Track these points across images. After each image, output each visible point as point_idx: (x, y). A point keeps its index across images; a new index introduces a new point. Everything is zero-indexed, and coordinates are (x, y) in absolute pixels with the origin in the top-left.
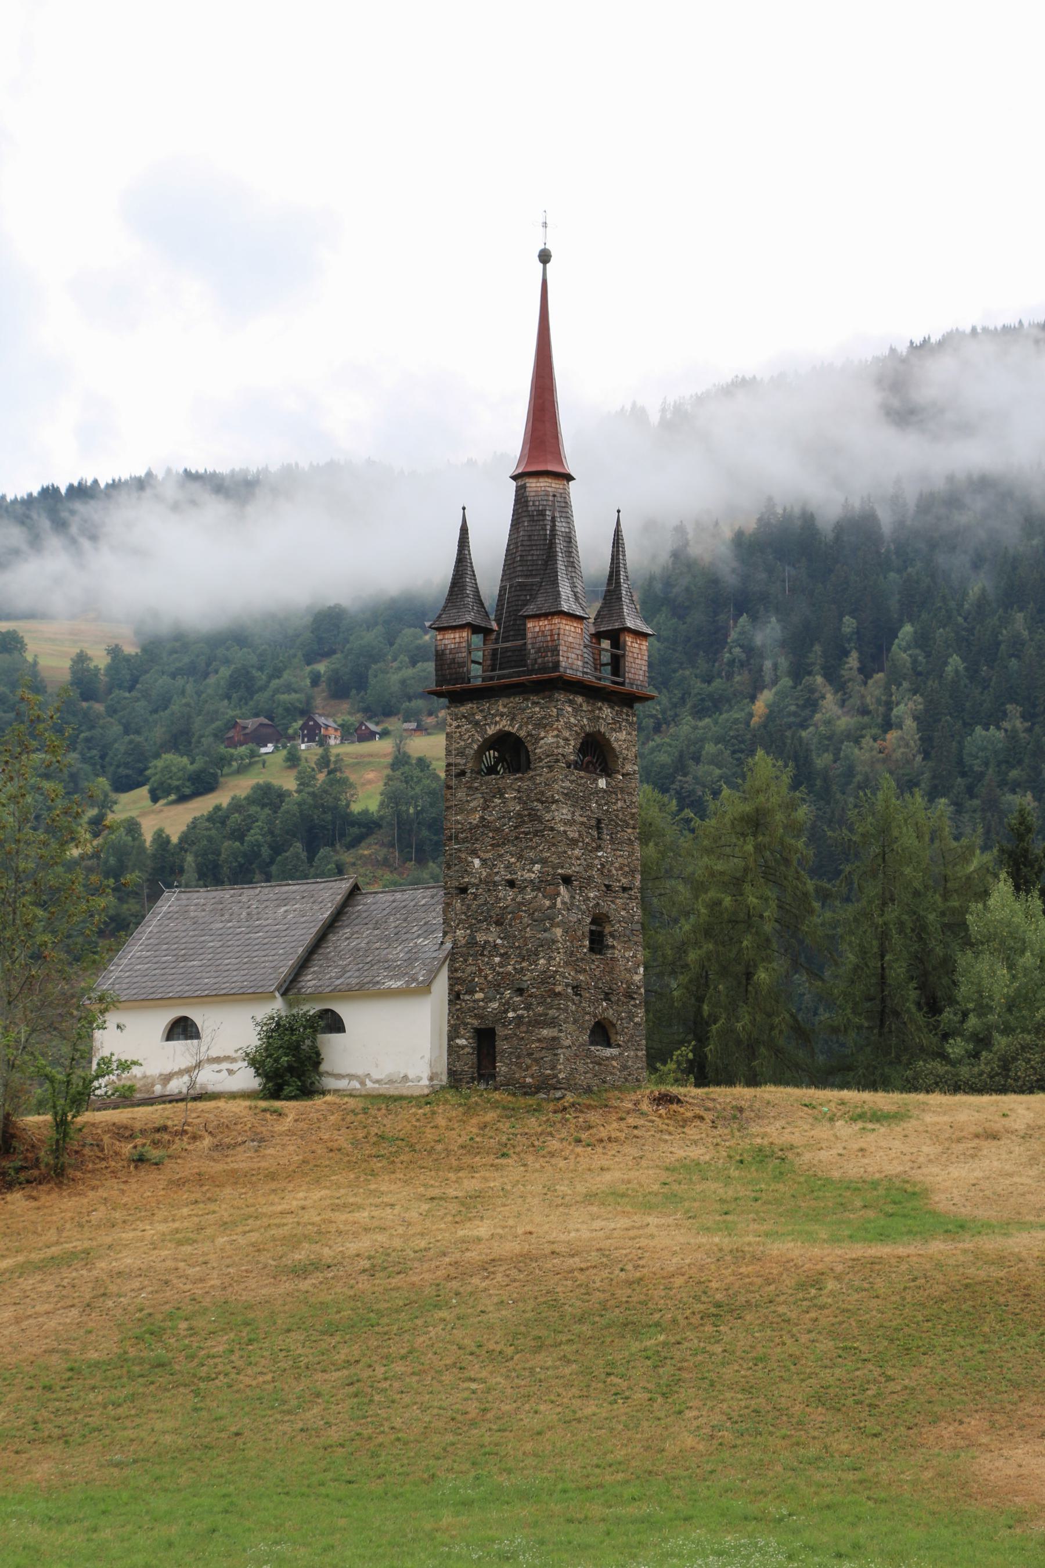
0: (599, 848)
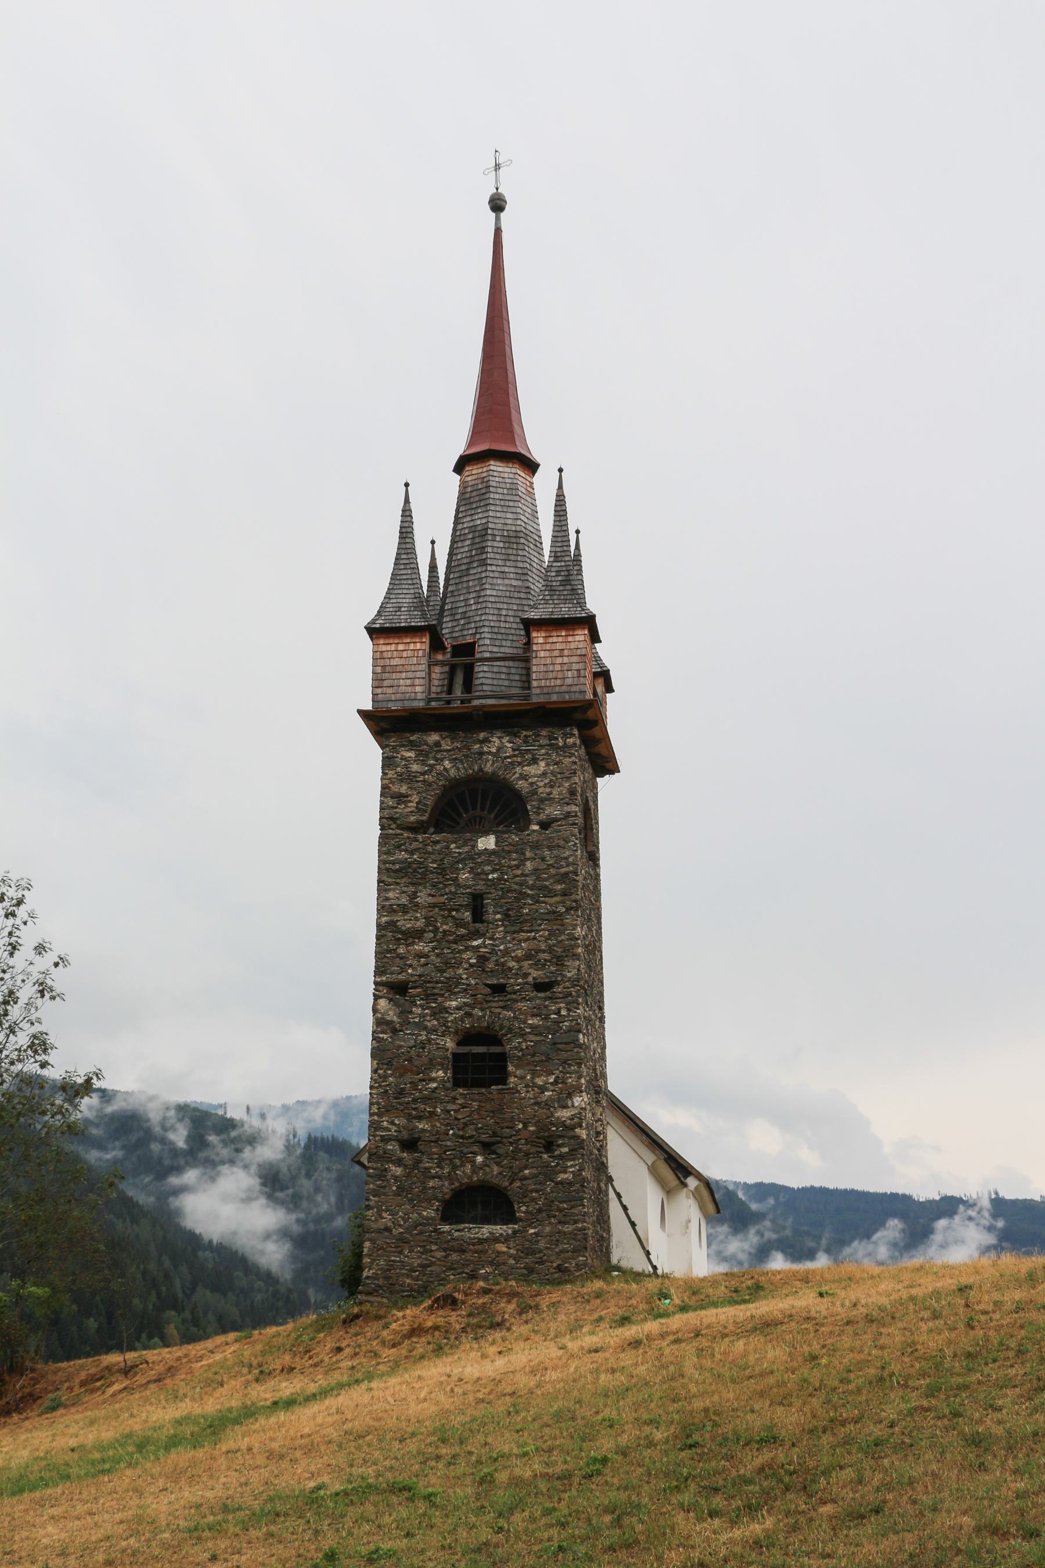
0: (476, 934)
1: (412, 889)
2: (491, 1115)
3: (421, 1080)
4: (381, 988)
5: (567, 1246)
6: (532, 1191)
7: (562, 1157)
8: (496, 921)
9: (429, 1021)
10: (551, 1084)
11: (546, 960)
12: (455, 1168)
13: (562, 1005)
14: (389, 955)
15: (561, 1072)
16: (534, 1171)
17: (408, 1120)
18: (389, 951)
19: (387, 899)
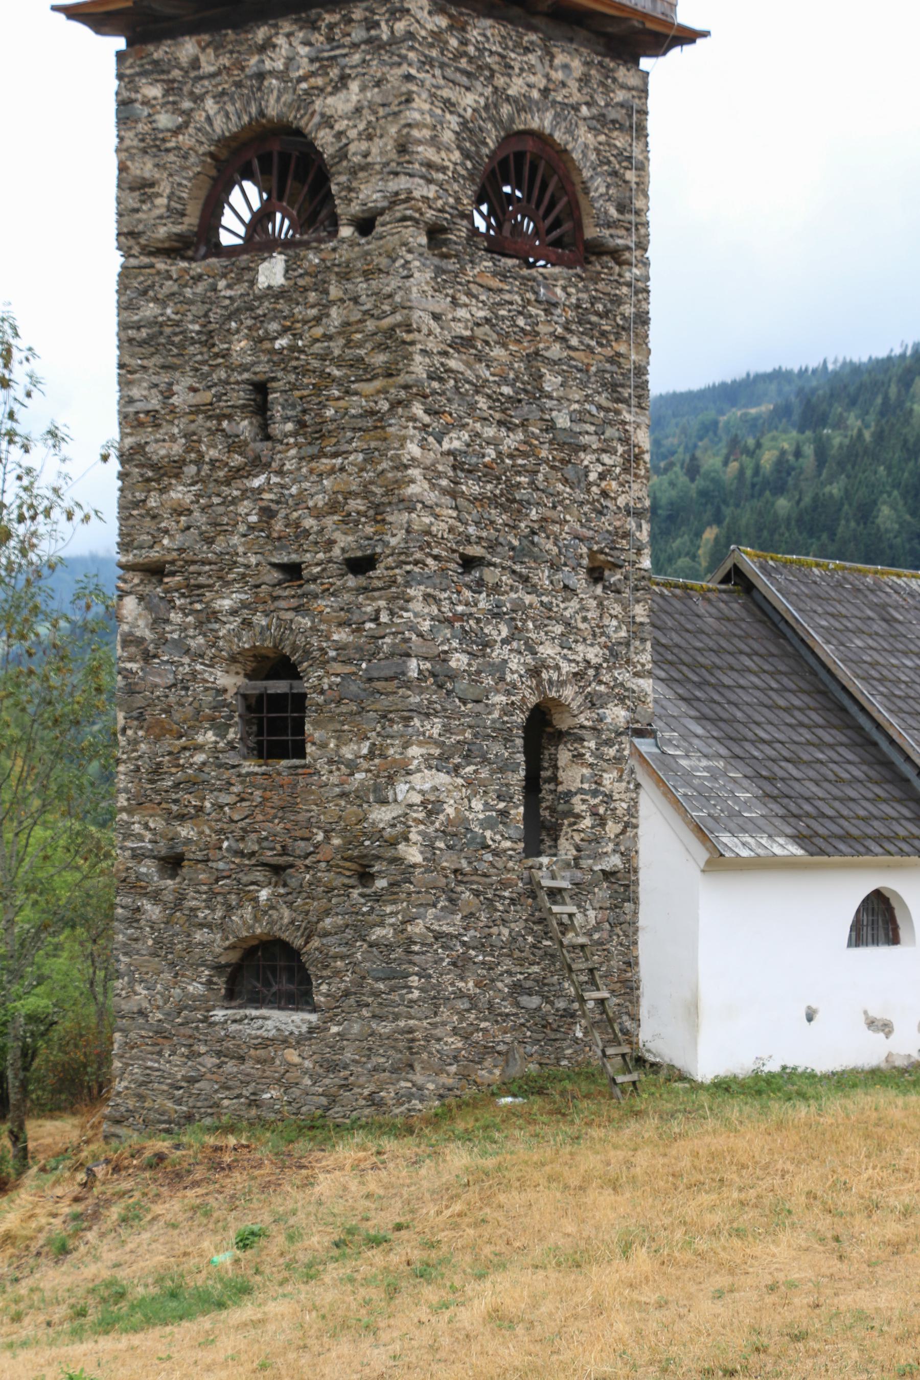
0: (257, 464)
1: (165, 378)
2: (280, 814)
3: (185, 748)
4: (129, 575)
5: (383, 1060)
6: (335, 957)
7: (378, 897)
8: (286, 436)
9: (194, 637)
10: (365, 757)
11: (358, 513)
12: (229, 909)
13: (382, 603)
14: (135, 512)
15: (379, 734)
16: (339, 920)
17: (166, 820)
18: (137, 504)
19: (131, 401)
